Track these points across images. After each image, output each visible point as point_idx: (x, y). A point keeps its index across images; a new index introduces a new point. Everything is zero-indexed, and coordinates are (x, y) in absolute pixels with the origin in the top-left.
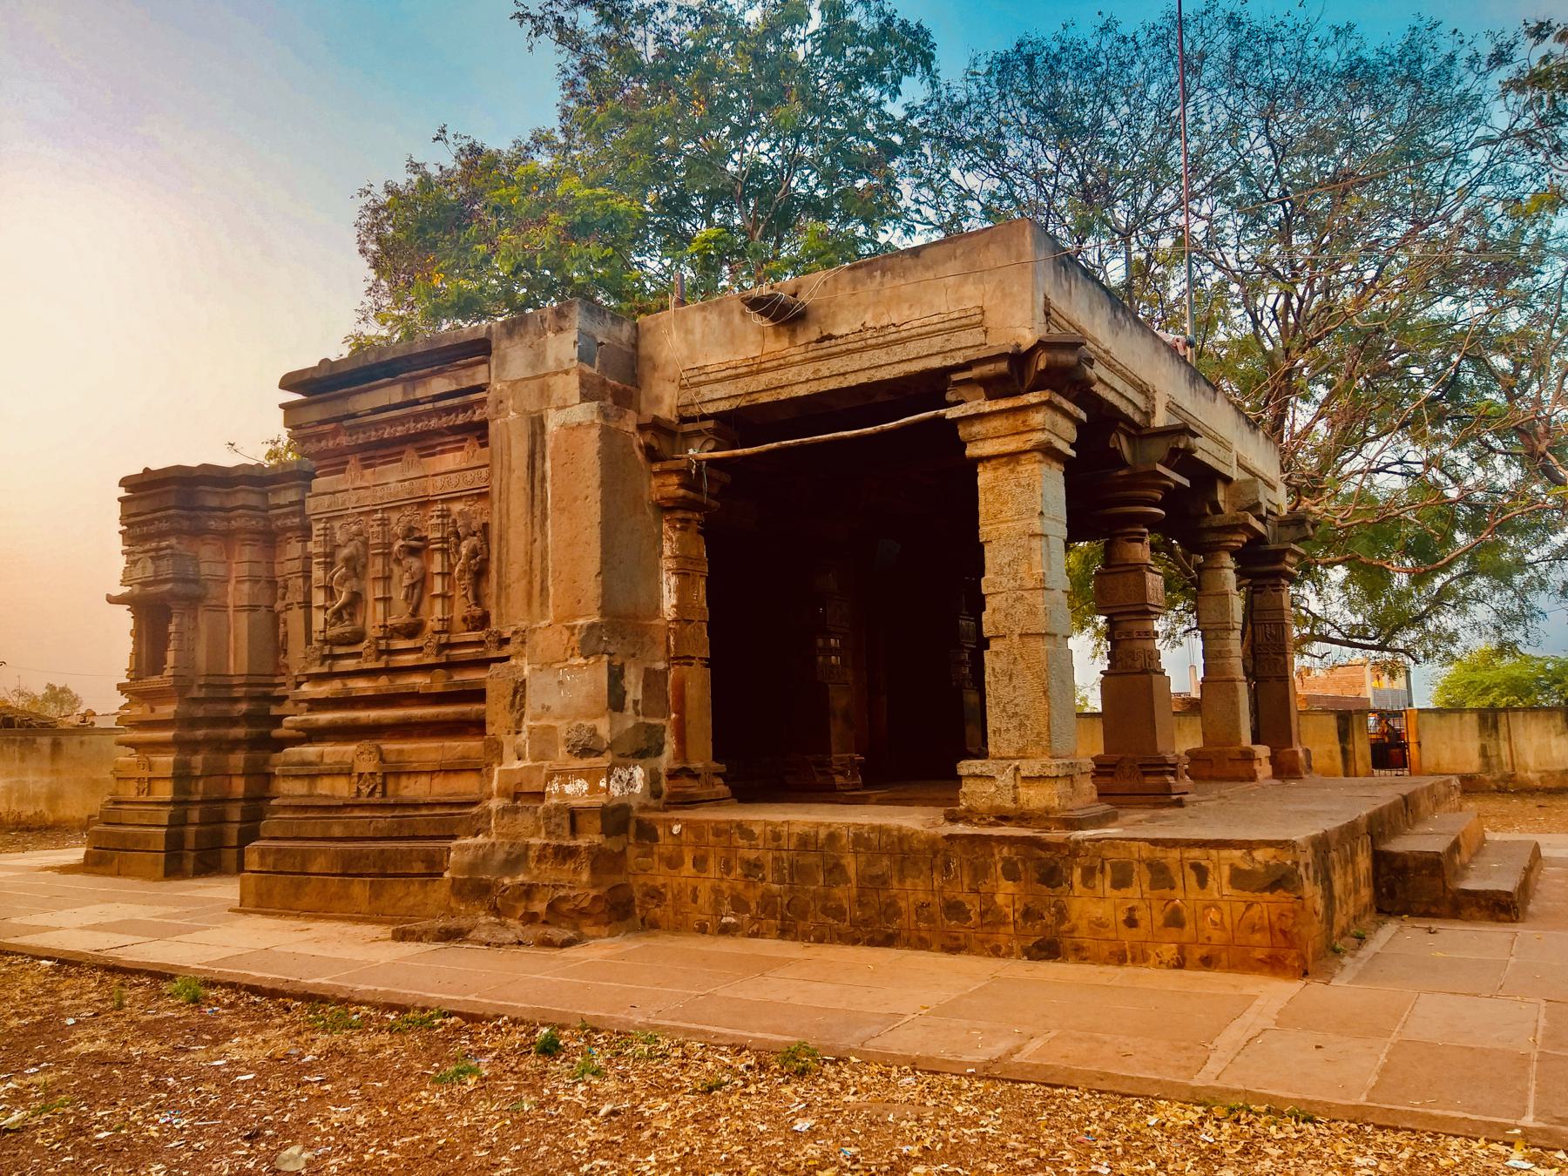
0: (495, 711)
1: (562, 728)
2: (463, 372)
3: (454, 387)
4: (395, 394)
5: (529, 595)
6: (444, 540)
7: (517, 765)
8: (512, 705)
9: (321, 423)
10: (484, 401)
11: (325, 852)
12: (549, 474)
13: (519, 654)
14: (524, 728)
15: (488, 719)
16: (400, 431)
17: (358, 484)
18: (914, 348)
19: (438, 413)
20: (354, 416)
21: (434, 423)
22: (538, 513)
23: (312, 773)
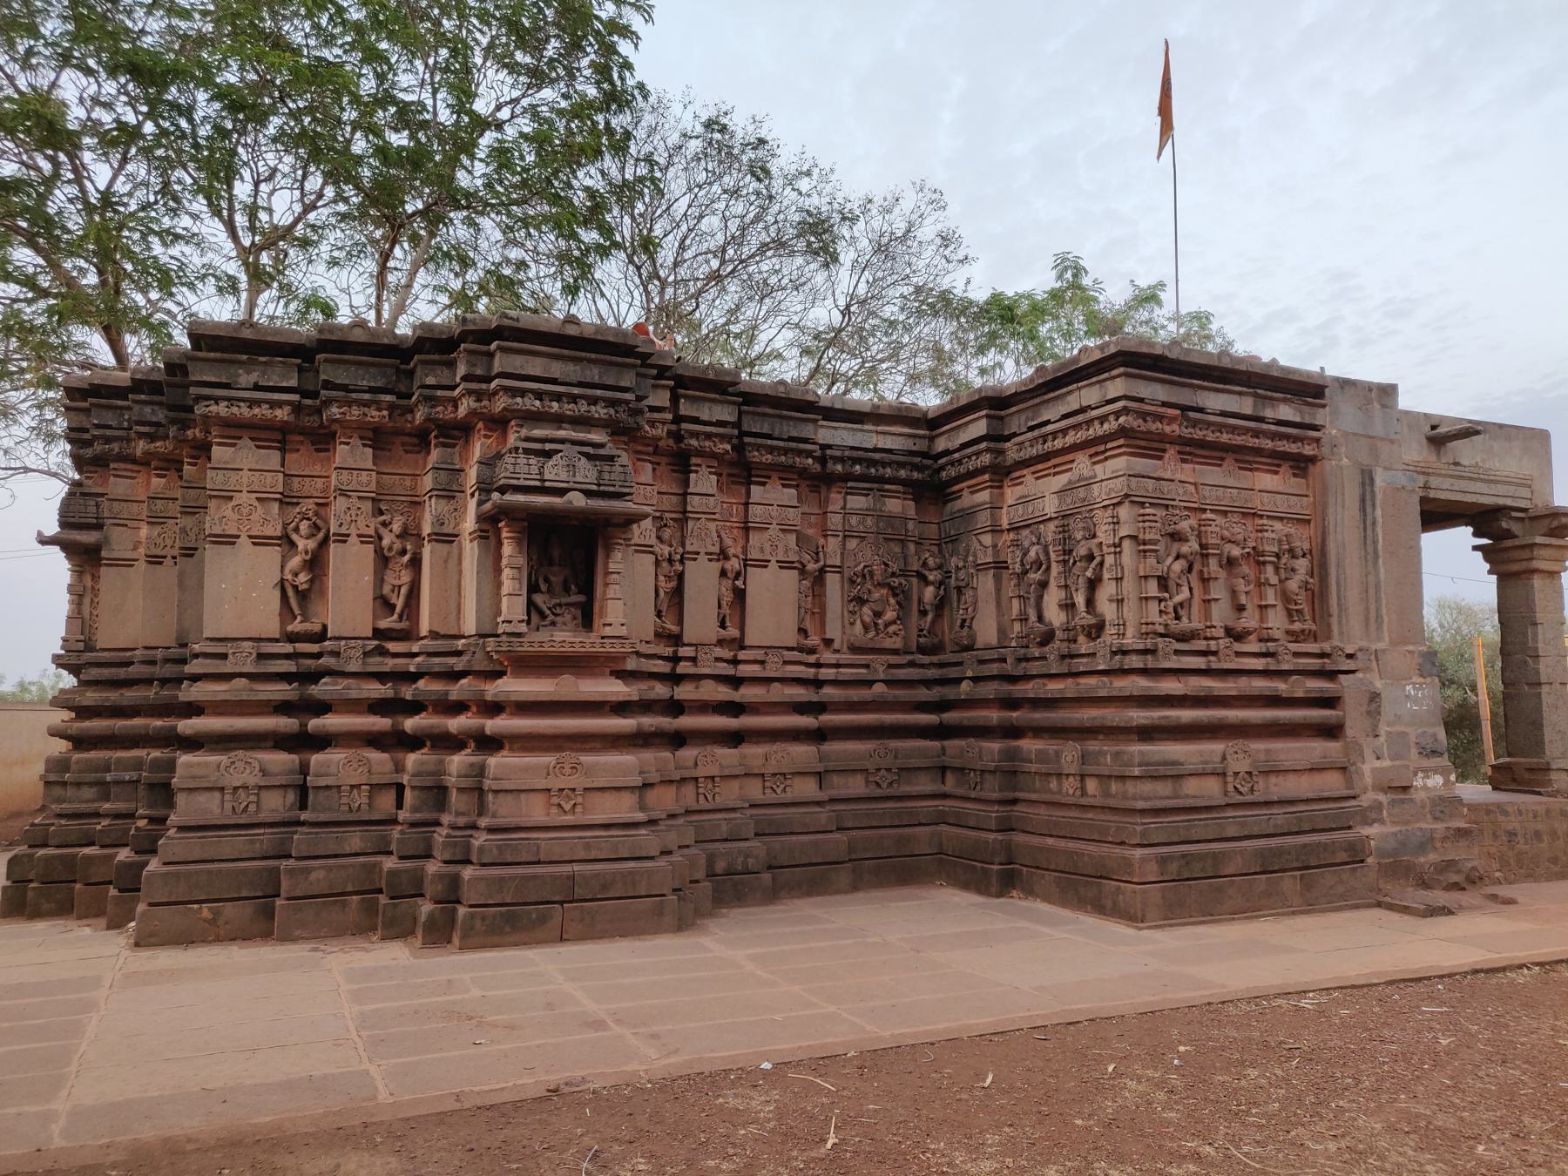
0: (1353, 716)
1: (1413, 733)
2: (1306, 409)
3: (1298, 419)
4: (1246, 405)
5: (1367, 619)
6: (1277, 556)
7: (1378, 764)
8: (1369, 713)
9: (1164, 404)
10: (1318, 440)
11: (1242, 852)
12: (1380, 520)
13: (1368, 669)
14: (1382, 733)
15: (1348, 724)
16: (1238, 440)
17: (1178, 476)
18: (1501, 489)
19: (1274, 436)
20: (1201, 410)
21: (1268, 444)
22: (1370, 549)
23: (1175, 774)
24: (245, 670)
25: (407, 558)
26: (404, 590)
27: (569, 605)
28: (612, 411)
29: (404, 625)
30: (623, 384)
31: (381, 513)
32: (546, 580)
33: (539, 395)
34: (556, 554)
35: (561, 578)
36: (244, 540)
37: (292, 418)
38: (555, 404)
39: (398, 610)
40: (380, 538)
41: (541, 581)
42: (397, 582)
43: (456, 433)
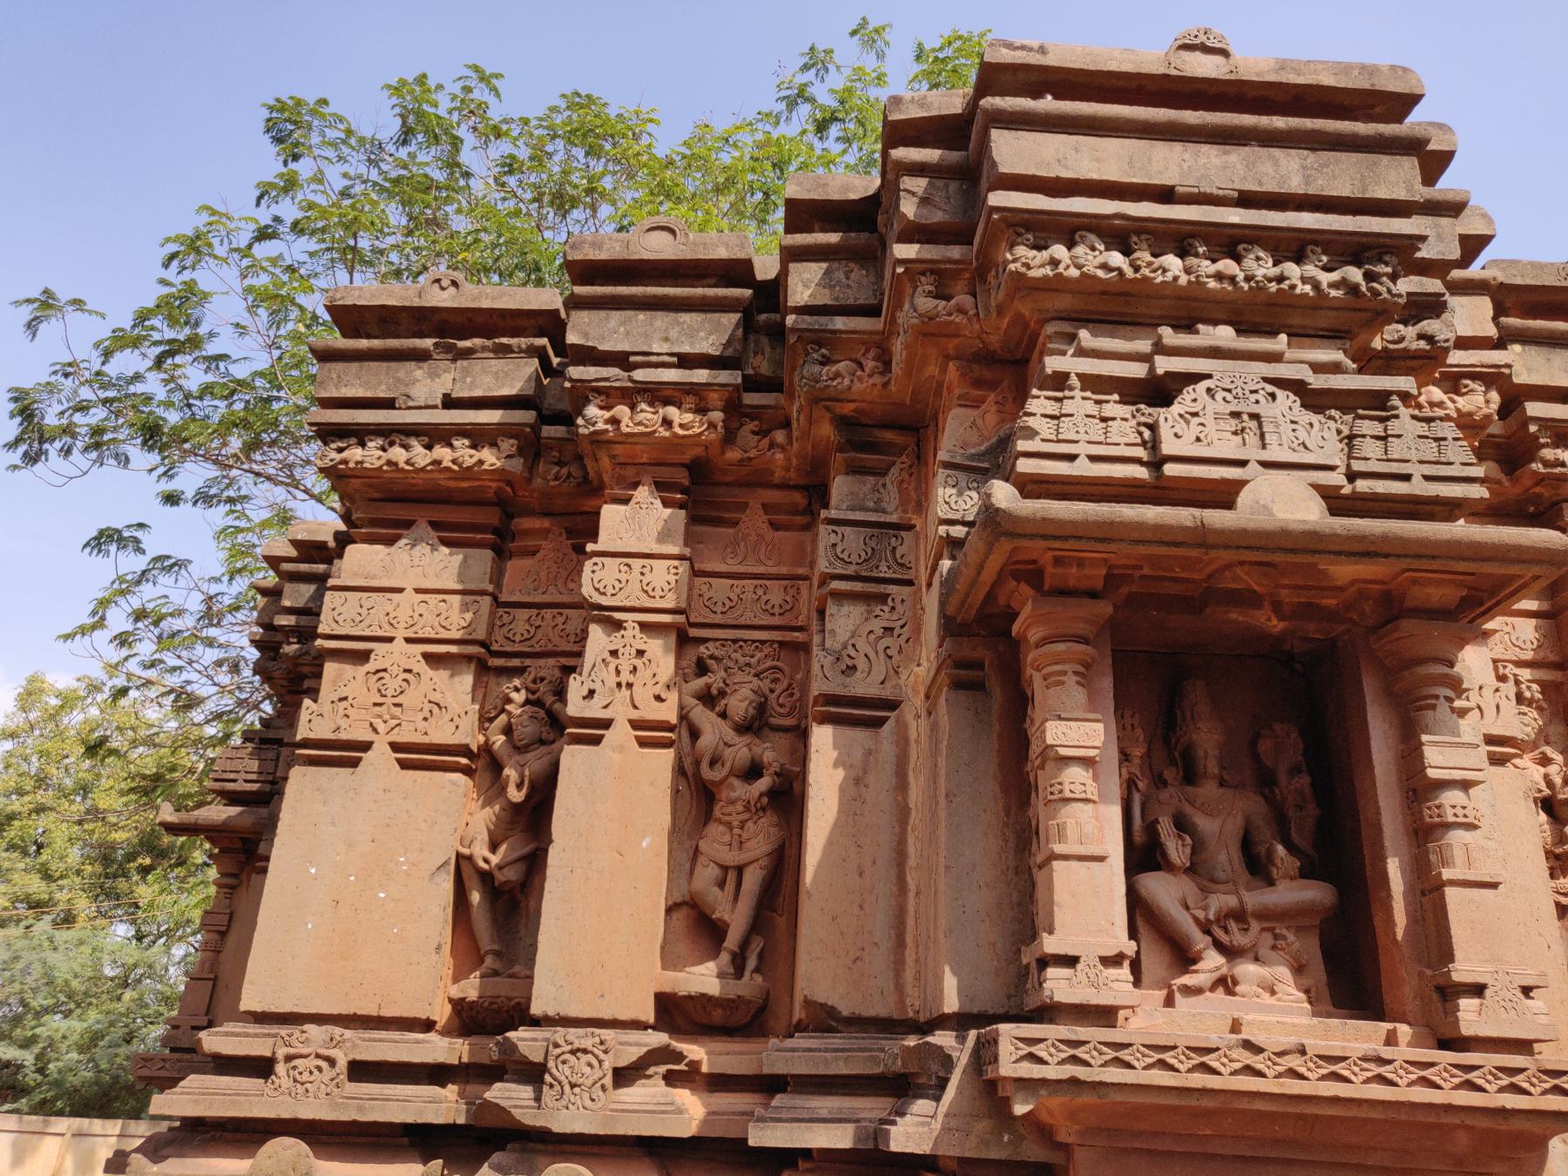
24: (308, 1111)
25: (763, 783)
26: (753, 879)
27: (1268, 916)
28: (1355, 274)
29: (749, 985)
30: (1381, 193)
31: (702, 669)
32: (1182, 825)
33: (1120, 236)
34: (1207, 739)
35: (1234, 827)
36: (380, 759)
37: (517, 465)
38: (1173, 262)
39: (732, 940)
40: (695, 734)
41: (1166, 829)
42: (732, 857)
43: (889, 436)
